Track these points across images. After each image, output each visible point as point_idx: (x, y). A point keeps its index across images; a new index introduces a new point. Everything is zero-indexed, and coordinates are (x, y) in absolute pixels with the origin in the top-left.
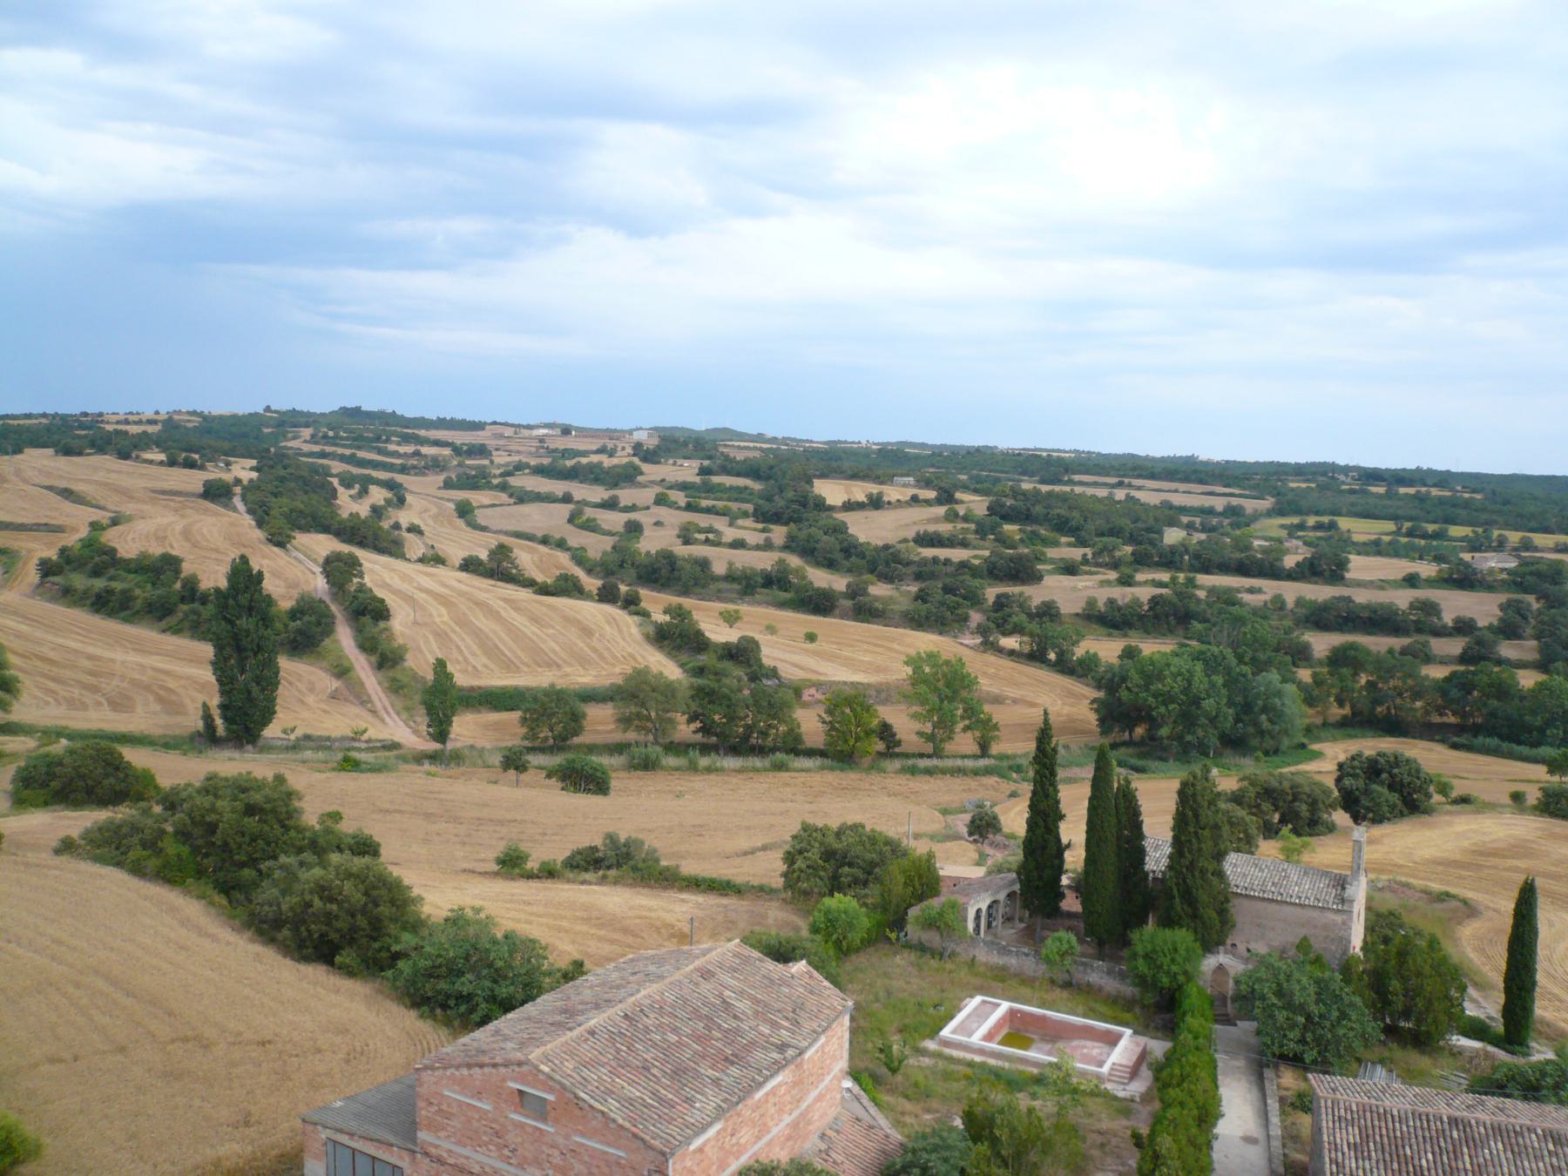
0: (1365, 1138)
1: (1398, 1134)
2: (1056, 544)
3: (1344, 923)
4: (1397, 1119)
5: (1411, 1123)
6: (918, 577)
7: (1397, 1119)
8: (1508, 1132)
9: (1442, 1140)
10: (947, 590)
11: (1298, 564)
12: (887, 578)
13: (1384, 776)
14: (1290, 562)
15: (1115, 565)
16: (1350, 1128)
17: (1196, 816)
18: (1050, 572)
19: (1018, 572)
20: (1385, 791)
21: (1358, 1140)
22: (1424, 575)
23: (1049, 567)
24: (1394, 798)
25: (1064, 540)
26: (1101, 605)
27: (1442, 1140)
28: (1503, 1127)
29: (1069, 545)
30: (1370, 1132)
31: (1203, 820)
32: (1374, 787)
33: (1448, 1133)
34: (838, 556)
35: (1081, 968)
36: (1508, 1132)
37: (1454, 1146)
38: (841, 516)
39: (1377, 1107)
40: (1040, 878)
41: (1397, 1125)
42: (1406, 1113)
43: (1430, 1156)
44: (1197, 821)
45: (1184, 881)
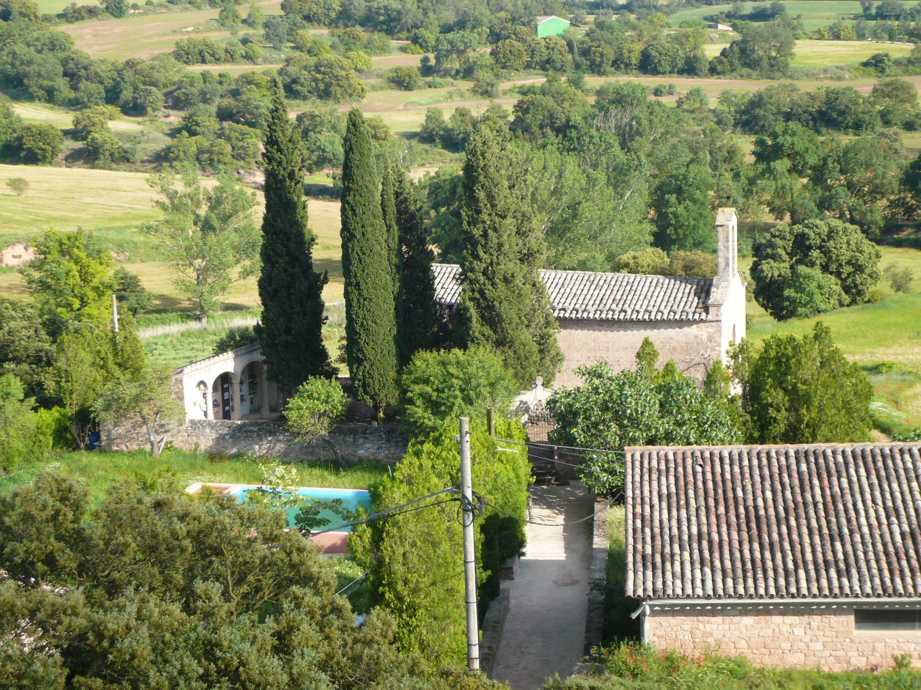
0: (682, 484)
1: (728, 476)
2: (384, 50)
3: (710, 339)
4: (727, 461)
5: (746, 463)
6: (176, 102)
7: (727, 461)
8: (874, 457)
9: (785, 475)
10: (224, 115)
11: (724, 53)
12: (134, 109)
13: (815, 253)
14: (712, 51)
15: (468, 72)
16: (663, 479)
17: (491, 197)
18: (374, 88)
19: (328, 85)
20: (816, 272)
21: (673, 489)
22: (895, 55)
23: (373, 81)
24: (833, 283)
25: (394, 43)
26: (447, 117)
27: (785, 475)
28: (868, 452)
29: (403, 50)
30: (691, 478)
31: (500, 204)
32: (802, 269)
33: (794, 467)
34: (62, 84)
35: (350, 439)
36: (874, 457)
37: (801, 481)
38: (64, 28)
39: (702, 453)
40: (288, 331)
41: (727, 468)
42: (740, 454)
43: (769, 495)
44: (493, 206)
45: (482, 292)
